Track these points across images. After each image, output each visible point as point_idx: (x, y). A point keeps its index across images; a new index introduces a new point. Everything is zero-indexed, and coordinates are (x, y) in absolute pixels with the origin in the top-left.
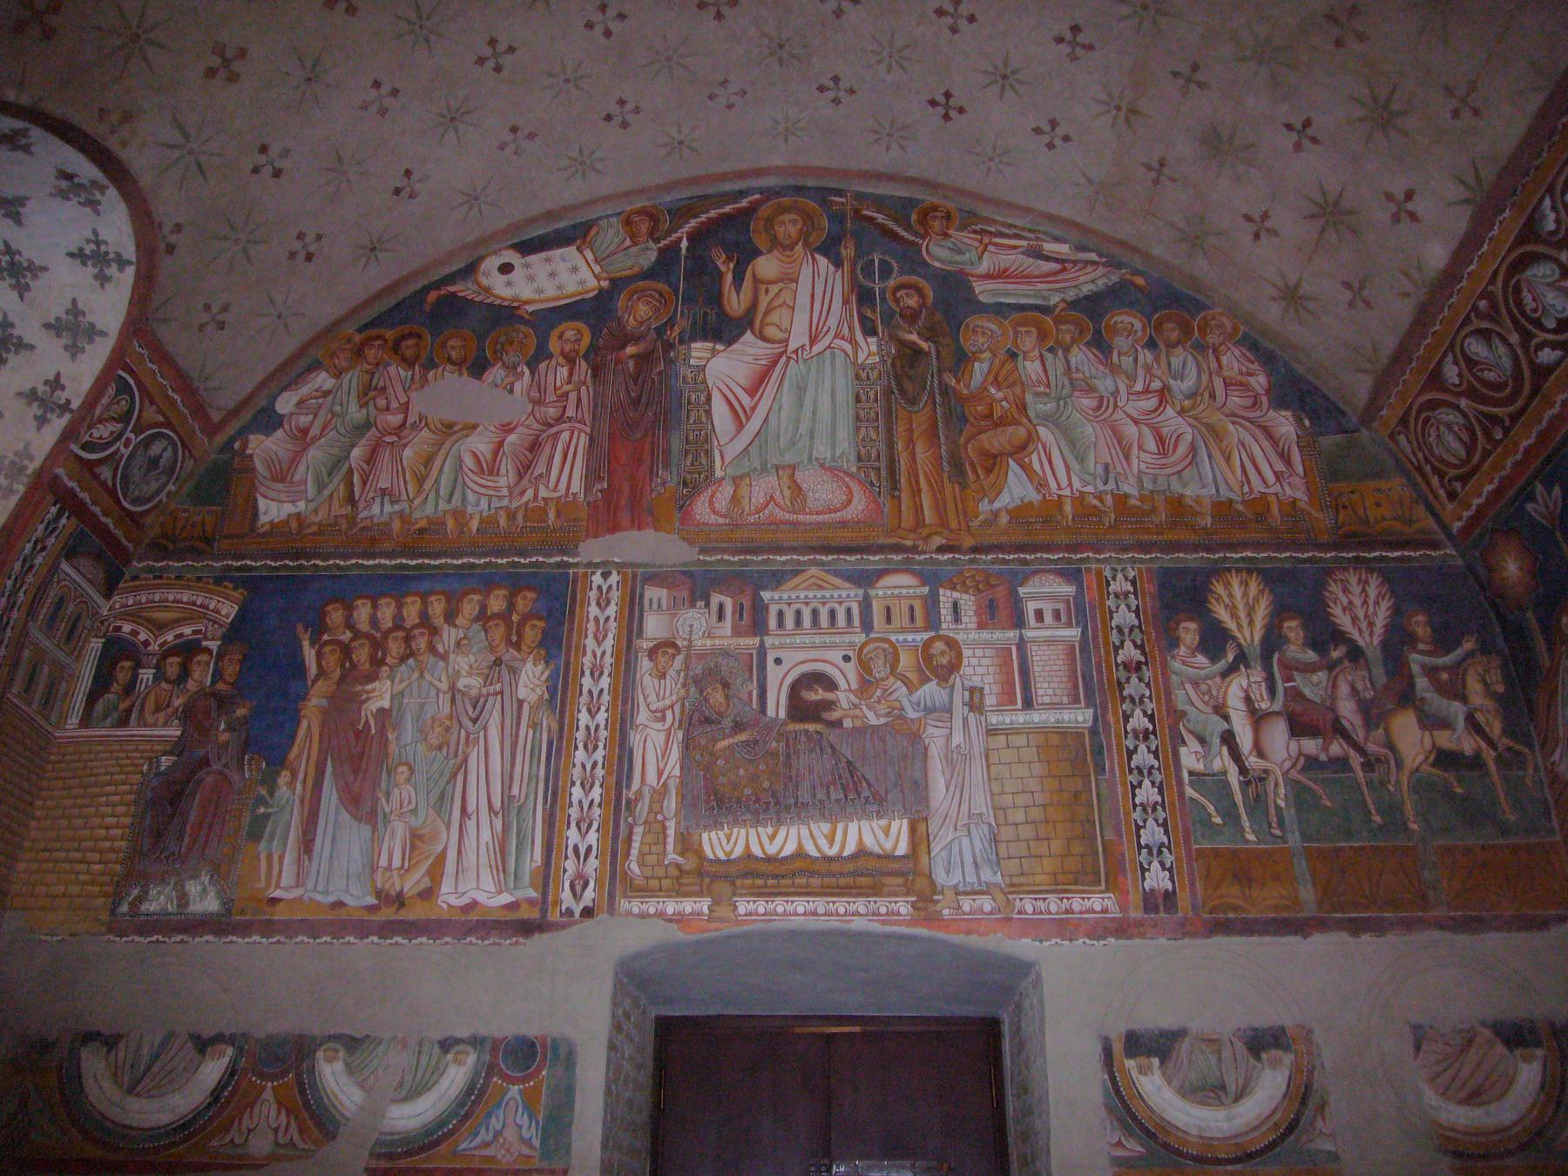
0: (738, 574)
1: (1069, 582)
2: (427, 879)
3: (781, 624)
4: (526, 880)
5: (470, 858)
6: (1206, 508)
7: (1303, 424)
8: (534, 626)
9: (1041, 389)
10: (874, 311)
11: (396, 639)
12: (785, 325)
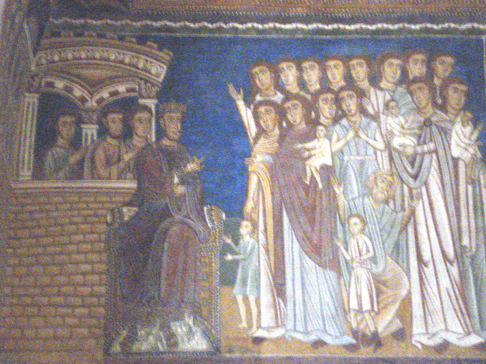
2: (398, 321)
5: (435, 303)
11: (326, 100)
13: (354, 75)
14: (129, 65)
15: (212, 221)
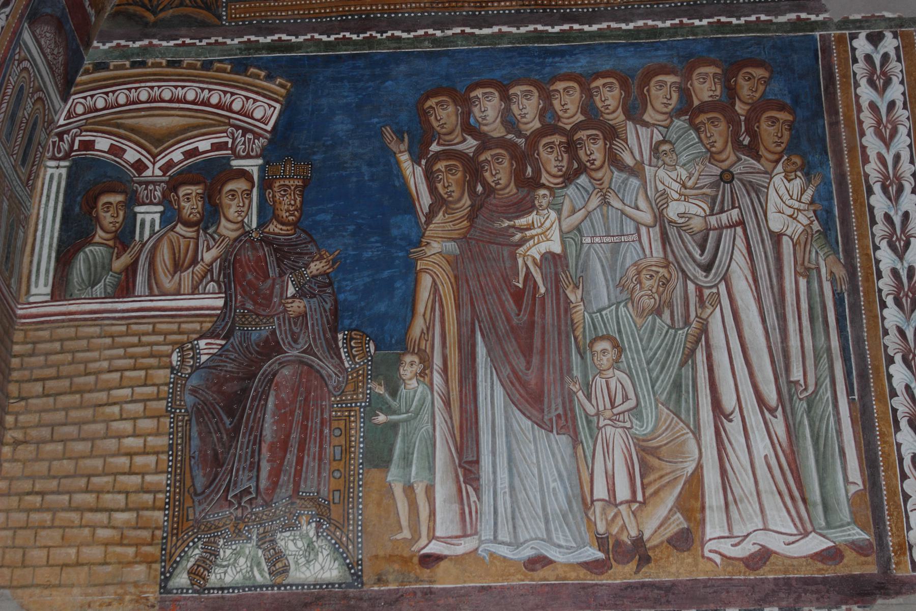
4: (845, 513)
5: (743, 482)
8: (774, 121)
11: (550, 145)
13: (600, 105)
14: (217, 106)
15: (352, 357)
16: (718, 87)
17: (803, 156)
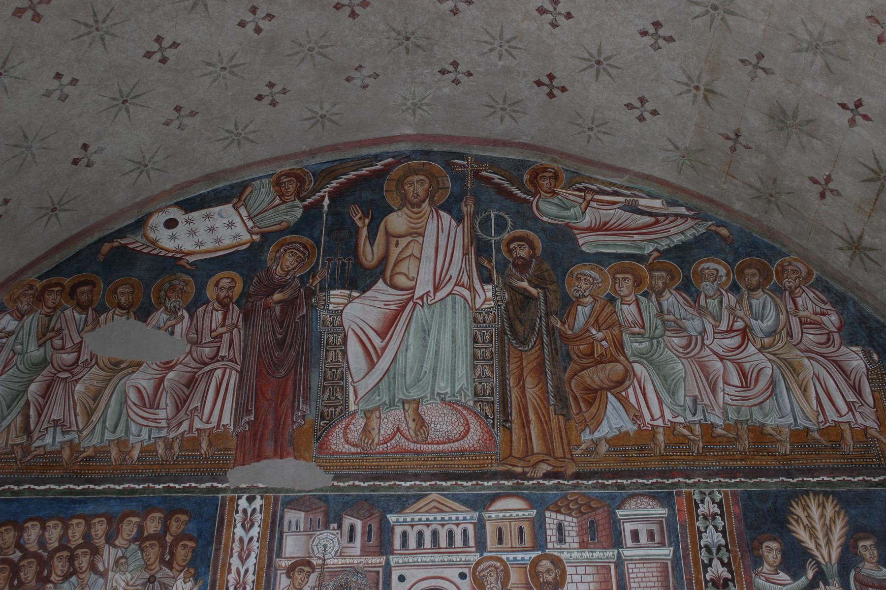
0: (366, 499)
1: (663, 506)
3: (404, 544)
6: (786, 435)
7: (872, 358)
8: (185, 546)
9: (637, 330)
10: (490, 261)
12: (413, 274)
13: (93, 533)
16: (160, 525)
17: (196, 569)
